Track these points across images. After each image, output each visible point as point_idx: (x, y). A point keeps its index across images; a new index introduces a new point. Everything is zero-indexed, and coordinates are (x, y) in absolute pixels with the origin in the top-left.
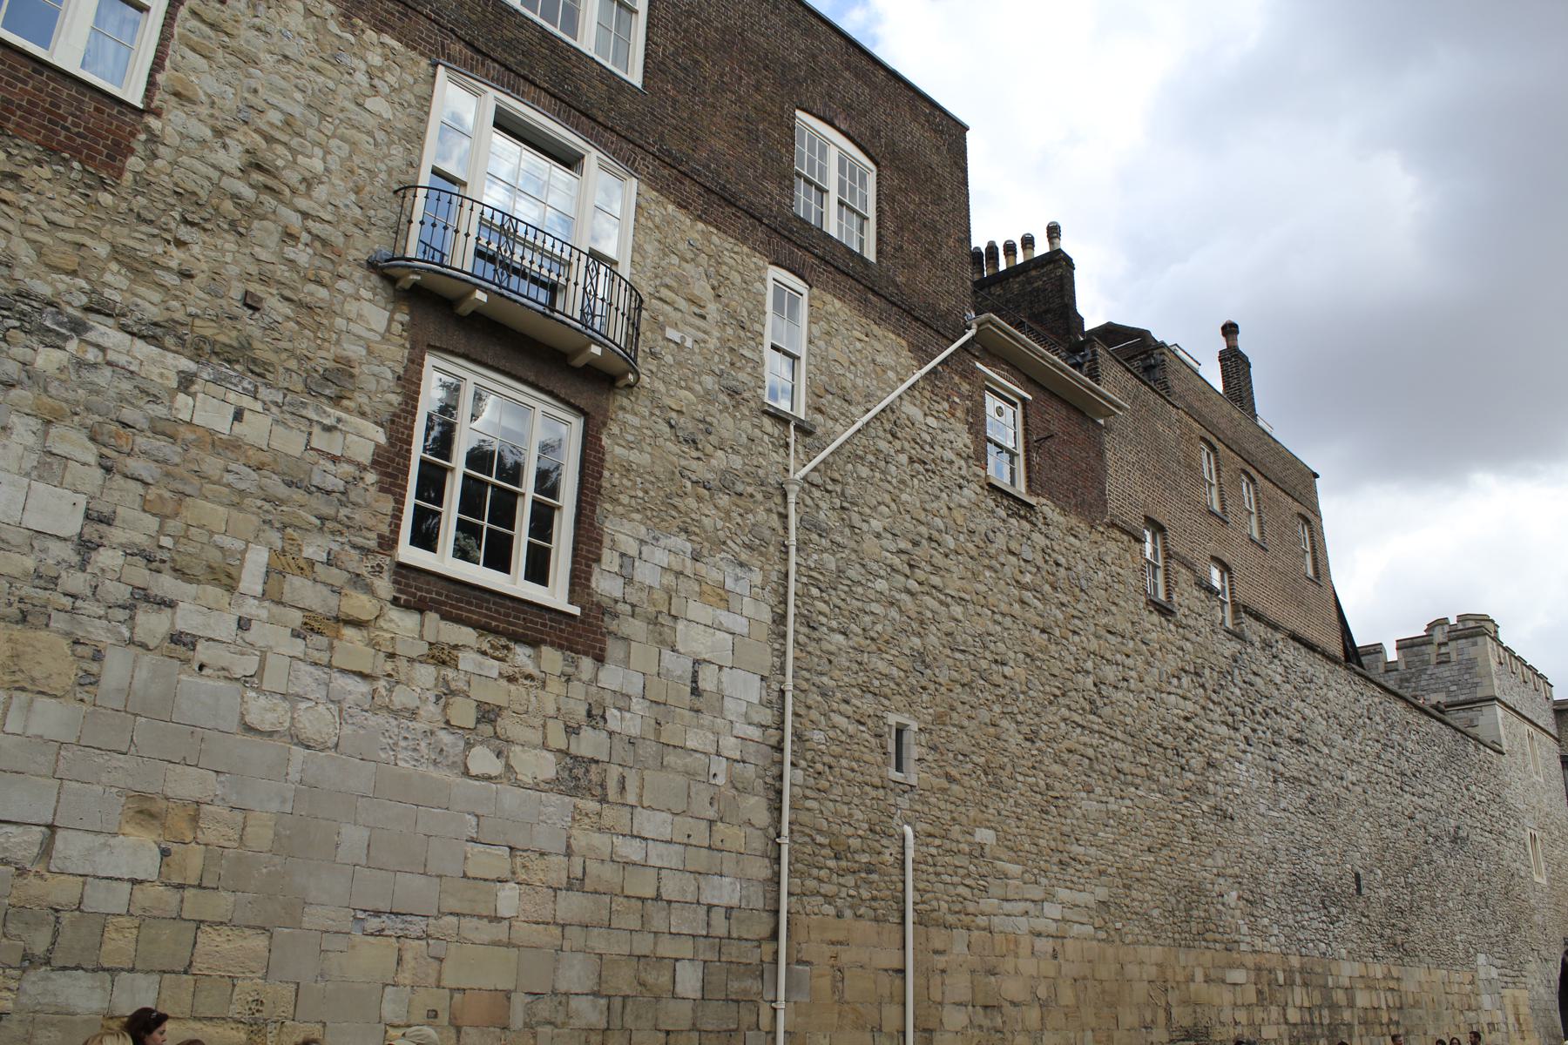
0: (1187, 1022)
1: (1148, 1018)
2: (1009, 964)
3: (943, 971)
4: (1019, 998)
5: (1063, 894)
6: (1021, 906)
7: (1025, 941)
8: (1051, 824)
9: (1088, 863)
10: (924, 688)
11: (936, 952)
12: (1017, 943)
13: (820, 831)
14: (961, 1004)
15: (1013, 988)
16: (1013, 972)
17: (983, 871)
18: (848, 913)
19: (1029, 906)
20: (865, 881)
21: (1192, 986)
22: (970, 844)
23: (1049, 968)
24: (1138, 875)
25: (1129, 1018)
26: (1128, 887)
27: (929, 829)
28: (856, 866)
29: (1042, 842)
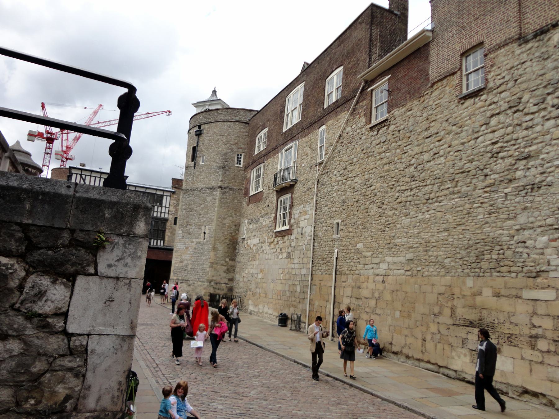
0: (472, 316)
1: (436, 310)
2: (365, 285)
3: (344, 287)
4: (368, 296)
5: (389, 259)
6: (371, 266)
7: (371, 278)
8: (385, 235)
9: (403, 245)
10: (344, 209)
11: (343, 282)
12: (368, 278)
13: (320, 256)
14: (348, 297)
15: (365, 293)
16: (366, 288)
17: (359, 256)
18: (324, 273)
19: (375, 266)
20: (327, 265)
21: (478, 299)
22: (354, 249)
23: (380, 286)
24: (434, 244)
25: (421, 308)
26: (426, 251)
27: (343, 248)
28: (325, 262)
29: (381, 242)
